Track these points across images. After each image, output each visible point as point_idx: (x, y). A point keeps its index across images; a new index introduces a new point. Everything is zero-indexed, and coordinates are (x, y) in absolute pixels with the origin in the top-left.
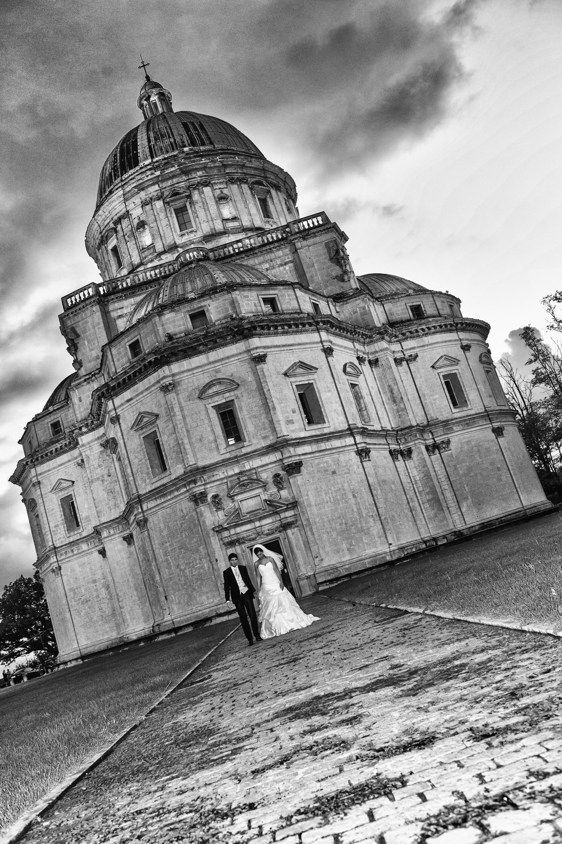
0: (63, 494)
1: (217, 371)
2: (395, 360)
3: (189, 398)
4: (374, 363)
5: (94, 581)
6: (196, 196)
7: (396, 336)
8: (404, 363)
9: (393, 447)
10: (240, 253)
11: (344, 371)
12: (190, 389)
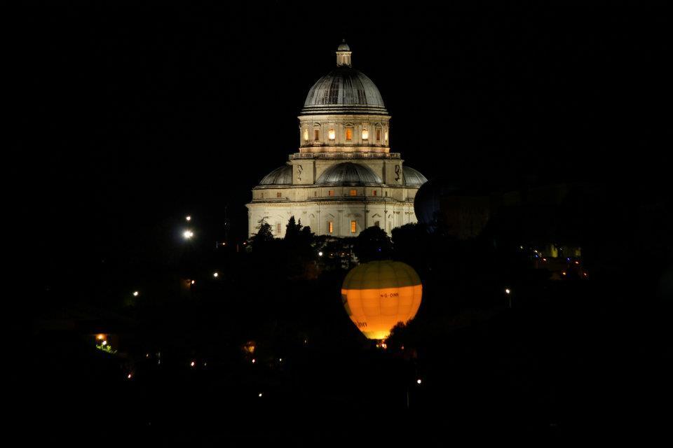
3: (345, 216)
4: (398, 213)
6: (356, 128)
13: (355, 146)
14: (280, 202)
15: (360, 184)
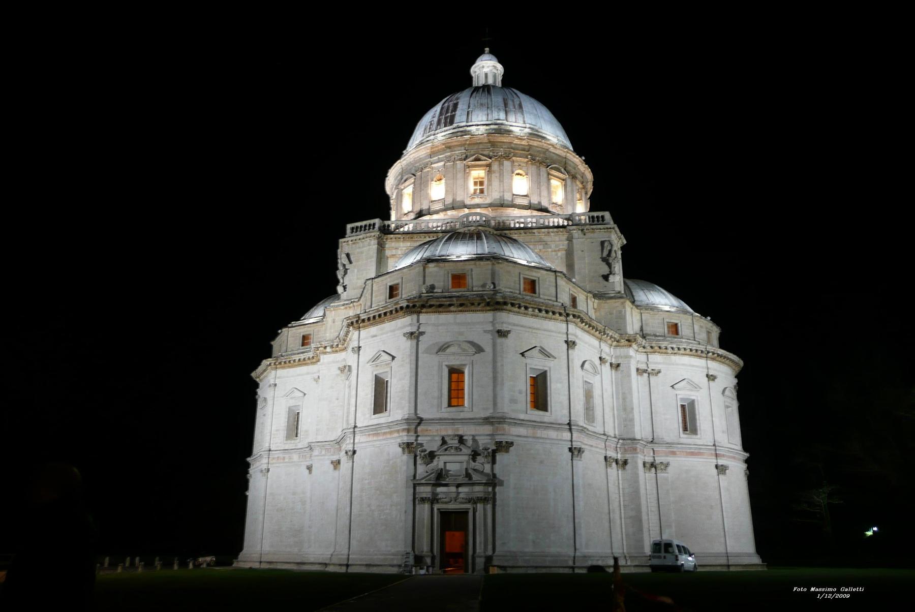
0: (292, 403)
1: (461, 334)
2: (638, 370)
3: (428, 351)
5: (294, 494)
6: (495, 167)
7: (644, 347)
8: (646, 375)
9: (611, 454)
10: (520, 228)
11: (582, 366)
12: (431, 343)
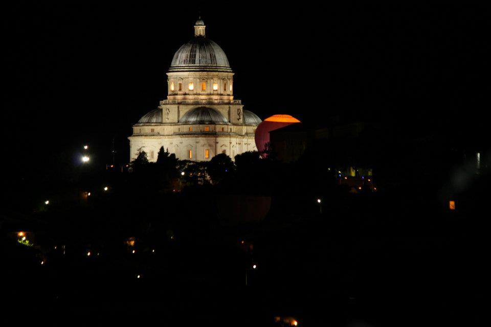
4: (240, 144)
6: (209, 81)
13: (208, 95)
14: (153, 135)
15: (212, 123)
